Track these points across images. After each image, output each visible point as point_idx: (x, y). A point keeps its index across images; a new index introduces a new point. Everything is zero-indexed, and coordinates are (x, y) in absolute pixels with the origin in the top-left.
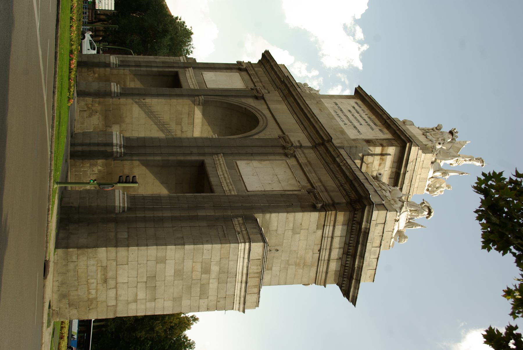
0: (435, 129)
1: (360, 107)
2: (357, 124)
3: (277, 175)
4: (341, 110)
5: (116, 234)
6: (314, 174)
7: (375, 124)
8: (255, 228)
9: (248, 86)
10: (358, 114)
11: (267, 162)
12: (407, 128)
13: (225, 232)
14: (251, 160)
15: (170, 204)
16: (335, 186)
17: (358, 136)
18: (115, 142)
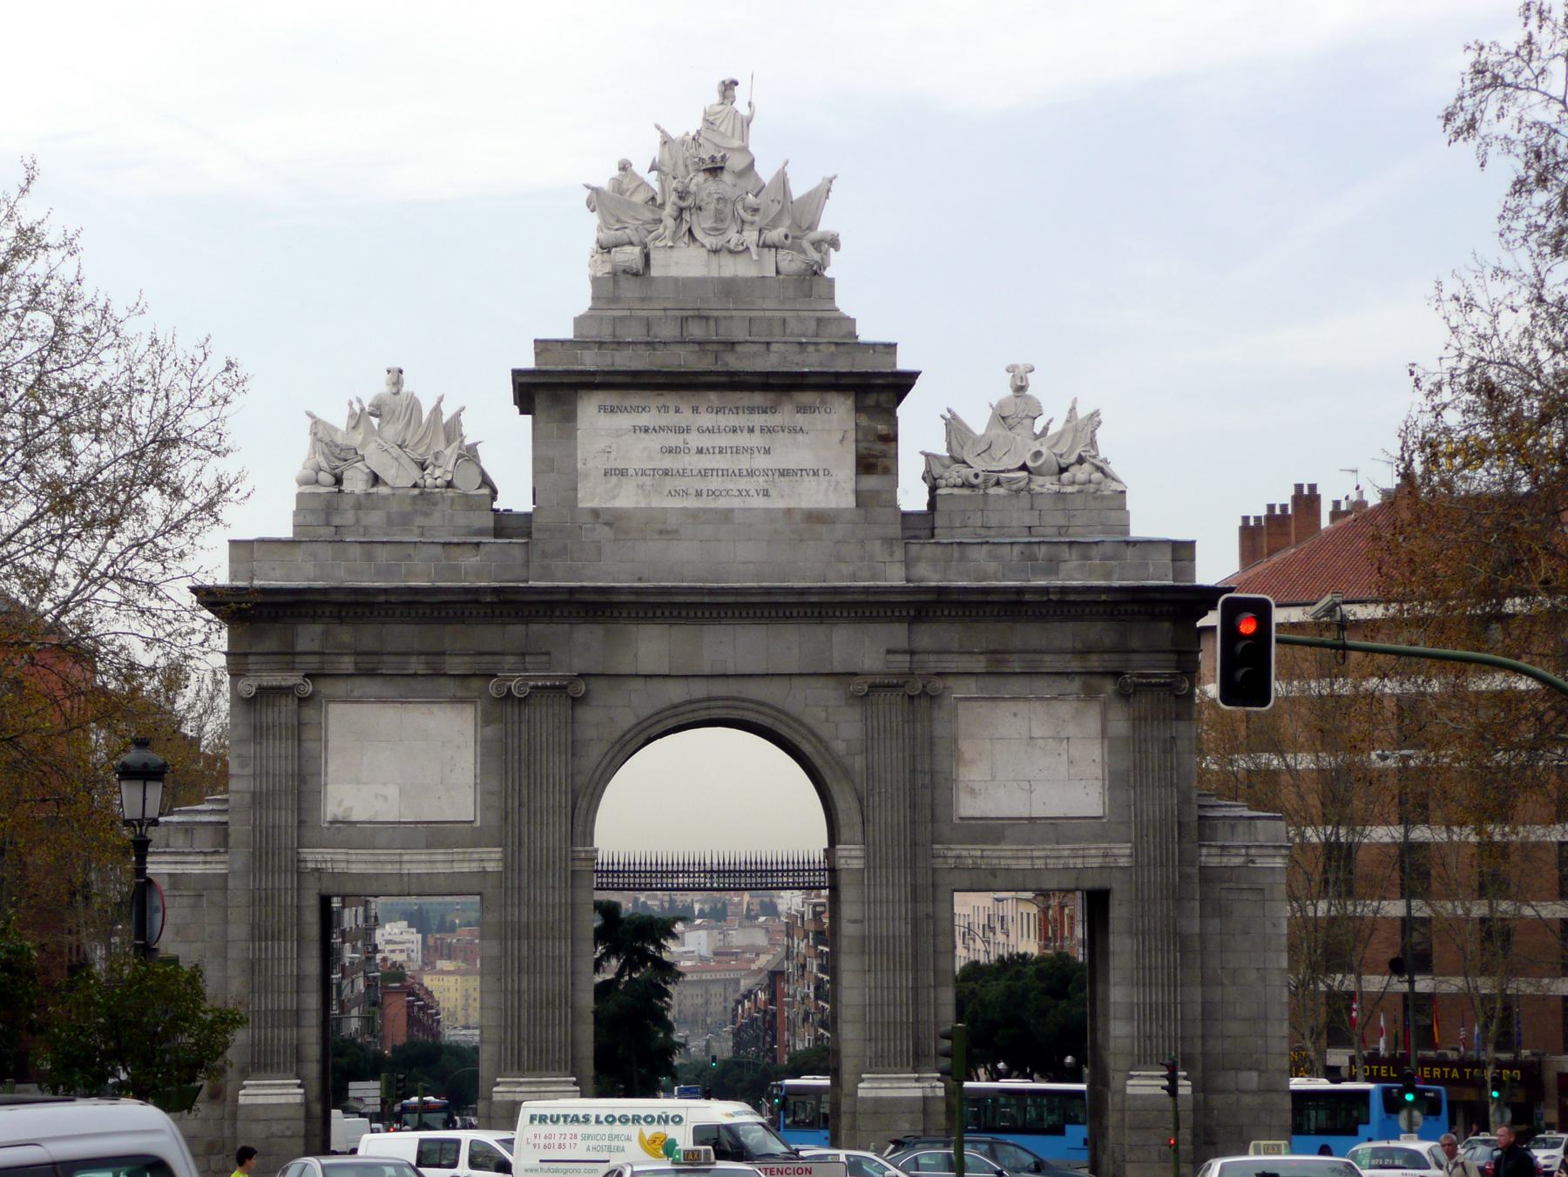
0: (683, 204)
1: (636, 409)
2: (761, 462)
3: (1031, 738)
4: (666, 473)
5: (1246, 1092)
6: (1048, 658)
7: (765, 412)
8: (1233, 827)
9: (451, 694)
10: (694, 433)
11: (965, 746)
12: (665, 279)
13: (1245, 886)
14: (951, 782)
15: (1169, 986)
16: (1100, 625)
17: (837, 483)
18: (919, 1093)
